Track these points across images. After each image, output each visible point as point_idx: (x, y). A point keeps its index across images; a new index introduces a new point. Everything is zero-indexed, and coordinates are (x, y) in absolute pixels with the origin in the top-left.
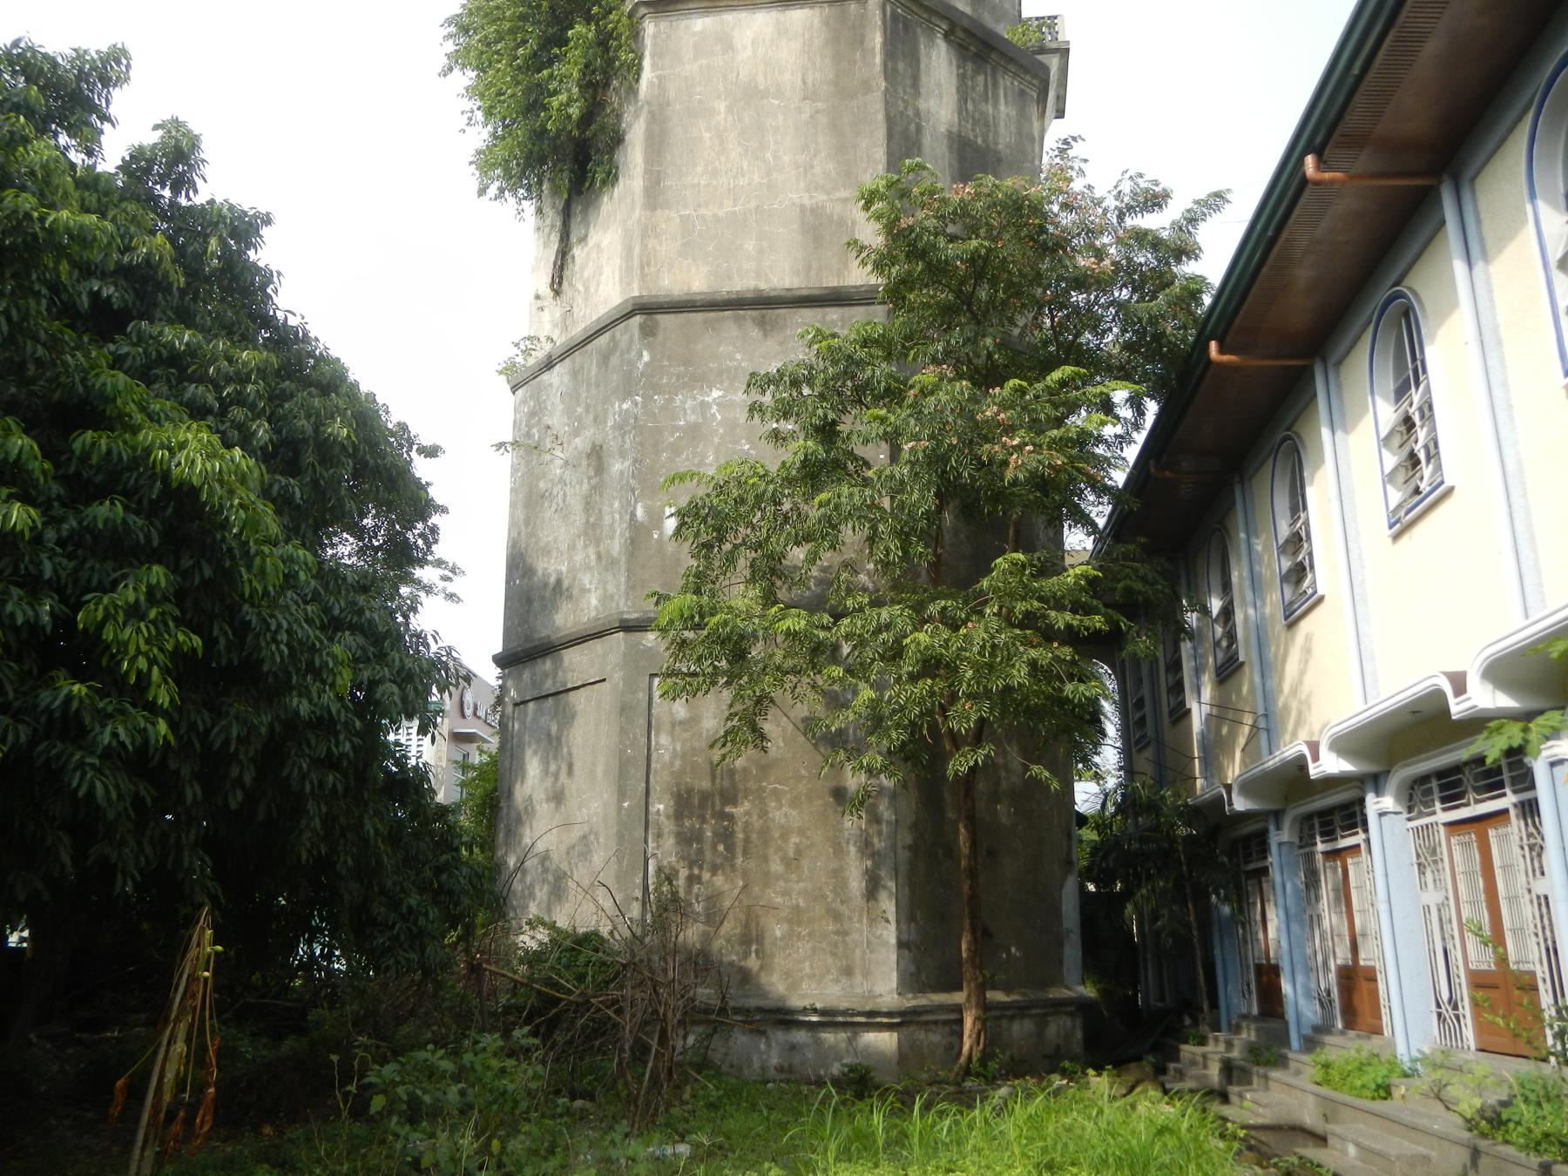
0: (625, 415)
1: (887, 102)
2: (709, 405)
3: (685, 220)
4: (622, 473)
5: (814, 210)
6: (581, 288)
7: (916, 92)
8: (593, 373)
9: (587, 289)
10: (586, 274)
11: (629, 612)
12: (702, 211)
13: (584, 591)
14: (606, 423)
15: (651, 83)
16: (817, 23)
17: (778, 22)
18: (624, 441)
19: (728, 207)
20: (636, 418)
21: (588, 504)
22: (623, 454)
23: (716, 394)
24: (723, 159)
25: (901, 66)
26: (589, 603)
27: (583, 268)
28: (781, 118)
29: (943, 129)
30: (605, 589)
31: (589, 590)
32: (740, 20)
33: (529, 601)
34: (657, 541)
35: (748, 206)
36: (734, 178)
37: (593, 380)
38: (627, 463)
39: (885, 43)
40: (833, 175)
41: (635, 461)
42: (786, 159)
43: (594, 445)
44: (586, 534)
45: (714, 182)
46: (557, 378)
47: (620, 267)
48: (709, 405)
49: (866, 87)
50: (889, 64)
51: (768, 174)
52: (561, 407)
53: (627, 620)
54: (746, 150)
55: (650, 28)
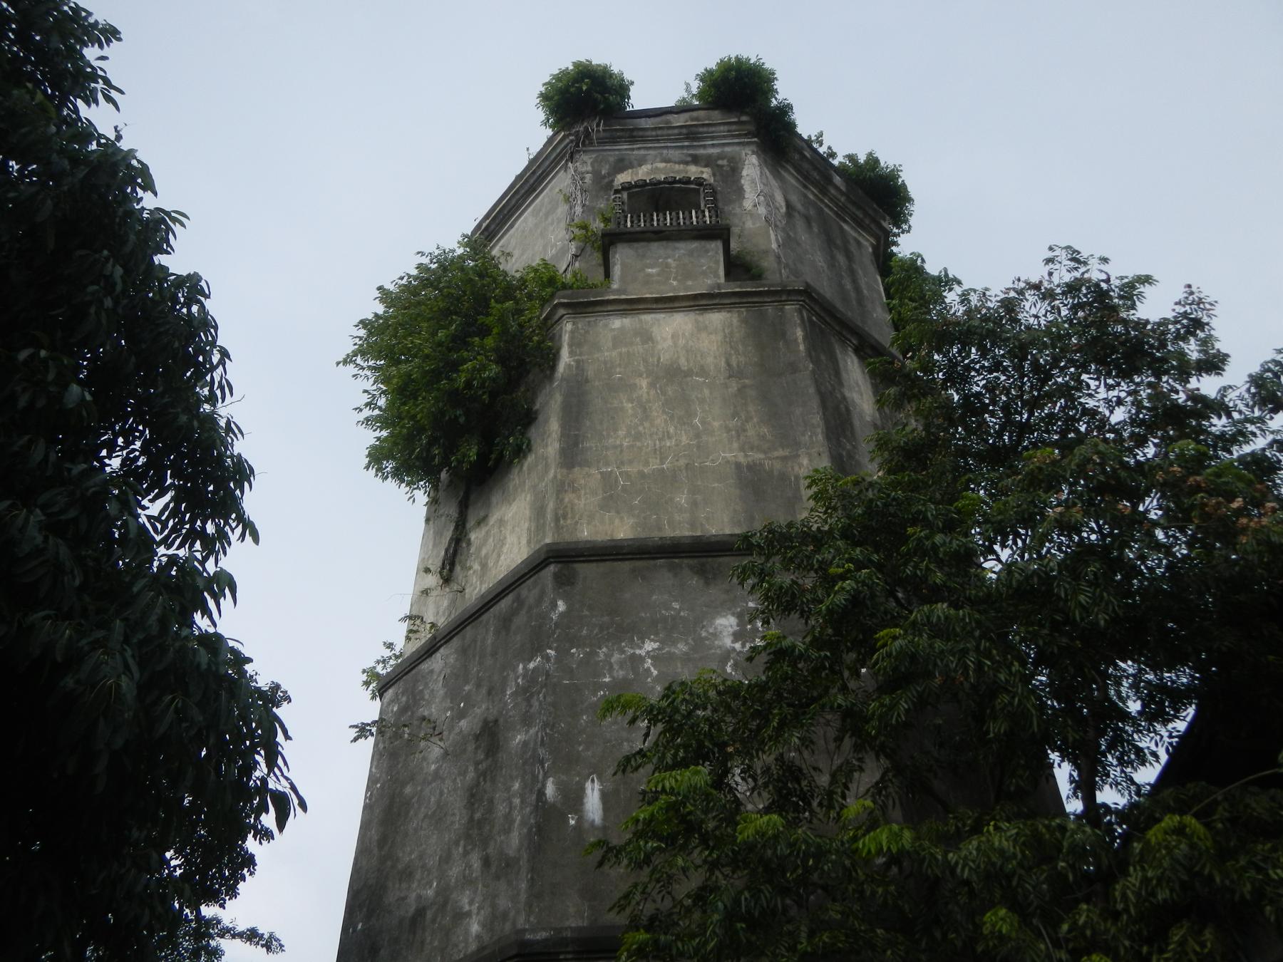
0: (531, 677)
1: (816, 381)
2: (641, 659)
3: (606, 477)
4: (525, 744)
5: (752, 467)
6: (476, 567)
7: (841, 384)
8: (489, 641)
9: (484, 566)
10: (484, 552)
11: (533, 930)
12: (626, 468)
13: (460, 916)
14: (504, 692)
15: (569, 366)
16: (735, 321)
17: (697, 322)
18: (531, 706)
19: (654, 465)
20: (548, 675)
21: (474, 796)
22: (527, 721)
23: (649, 646)
24: (647, 424)
25: (823, 357)
26: (467, 932)
27: (479, 549)
28: (706, 392)
29: (868, 419)
30: (494, 906)
31: (469, 914)
32: (658, 320)
33: (374, 950)
34: (575, 828)
35: (676, 463)
36: (660, 440)
37: (489, 649)
38: (532, 731)
39: (805, 338)
40: (769, 437)
41: (545, 725)
42: (716, 424)
43: (486, 722)
44: (468, 837)
45: (638, 444)
46: (437, 663)
47: (529, 529)
48: (641, 659)
49: (793, 368)
50: (813, 354)
51: (698, 436)
52: (442, 692)
53: (531, 943)
54: (672, 418)
55: (568, 326)
